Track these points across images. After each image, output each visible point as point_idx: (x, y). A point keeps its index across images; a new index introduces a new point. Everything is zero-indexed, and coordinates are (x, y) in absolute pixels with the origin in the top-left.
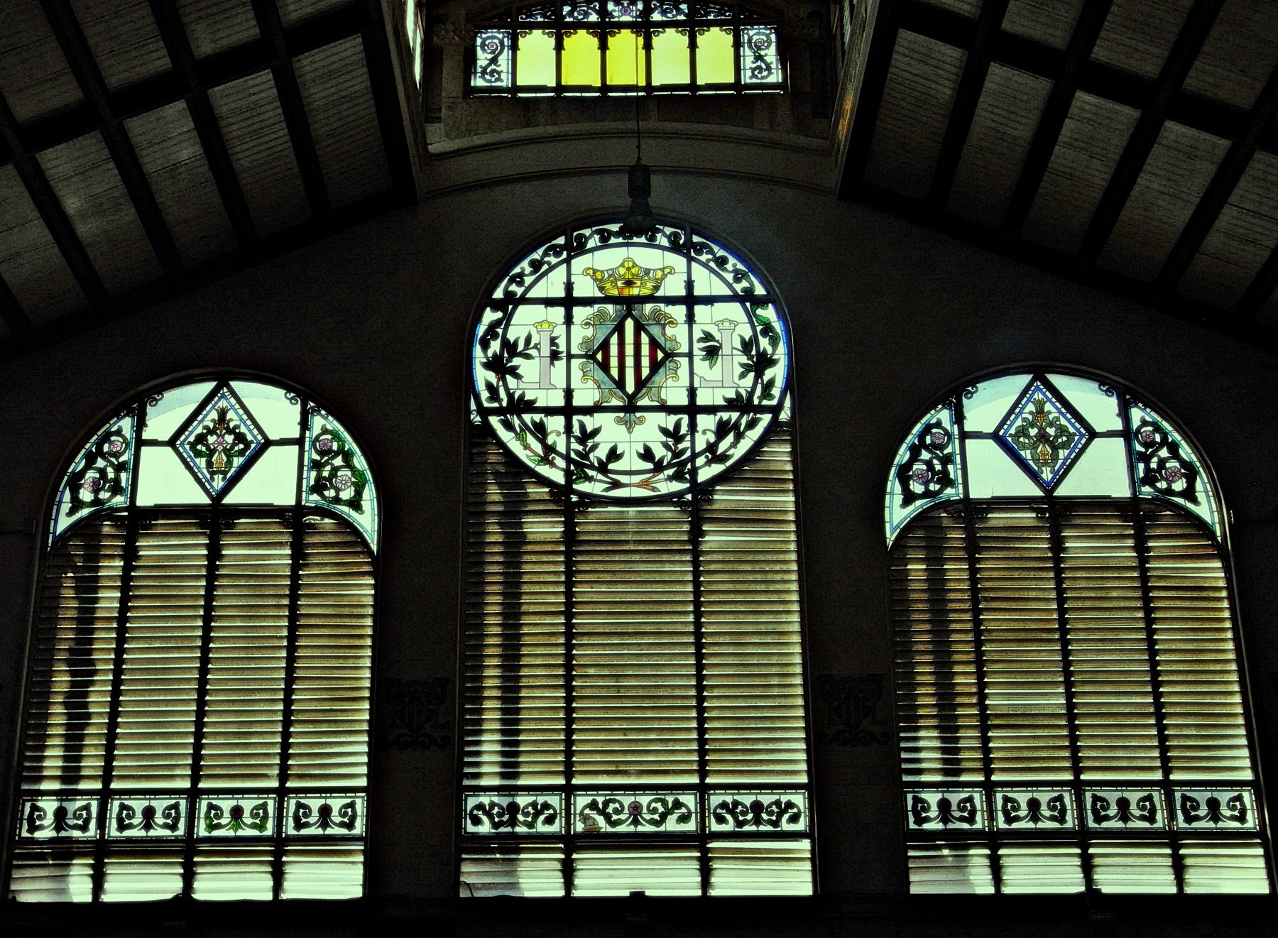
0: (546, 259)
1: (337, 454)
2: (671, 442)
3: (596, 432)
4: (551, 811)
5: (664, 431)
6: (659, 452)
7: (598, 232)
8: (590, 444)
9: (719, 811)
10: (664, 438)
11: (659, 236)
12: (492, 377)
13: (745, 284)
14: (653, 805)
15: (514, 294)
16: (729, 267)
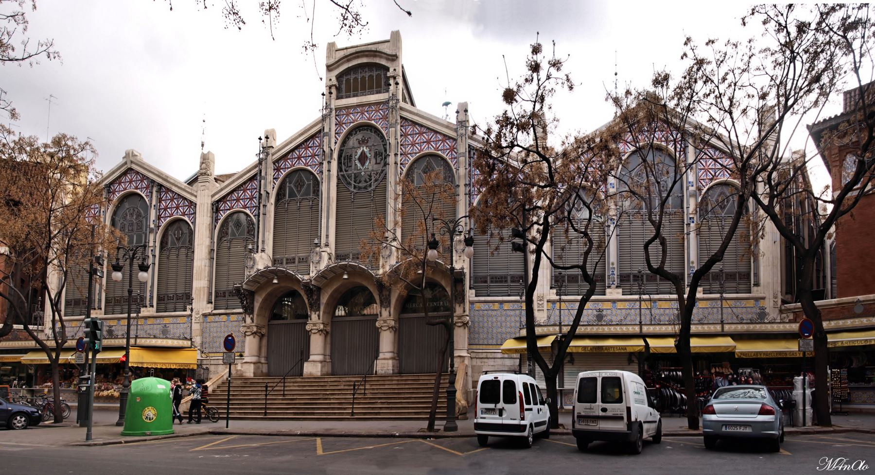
6: (368, 180)
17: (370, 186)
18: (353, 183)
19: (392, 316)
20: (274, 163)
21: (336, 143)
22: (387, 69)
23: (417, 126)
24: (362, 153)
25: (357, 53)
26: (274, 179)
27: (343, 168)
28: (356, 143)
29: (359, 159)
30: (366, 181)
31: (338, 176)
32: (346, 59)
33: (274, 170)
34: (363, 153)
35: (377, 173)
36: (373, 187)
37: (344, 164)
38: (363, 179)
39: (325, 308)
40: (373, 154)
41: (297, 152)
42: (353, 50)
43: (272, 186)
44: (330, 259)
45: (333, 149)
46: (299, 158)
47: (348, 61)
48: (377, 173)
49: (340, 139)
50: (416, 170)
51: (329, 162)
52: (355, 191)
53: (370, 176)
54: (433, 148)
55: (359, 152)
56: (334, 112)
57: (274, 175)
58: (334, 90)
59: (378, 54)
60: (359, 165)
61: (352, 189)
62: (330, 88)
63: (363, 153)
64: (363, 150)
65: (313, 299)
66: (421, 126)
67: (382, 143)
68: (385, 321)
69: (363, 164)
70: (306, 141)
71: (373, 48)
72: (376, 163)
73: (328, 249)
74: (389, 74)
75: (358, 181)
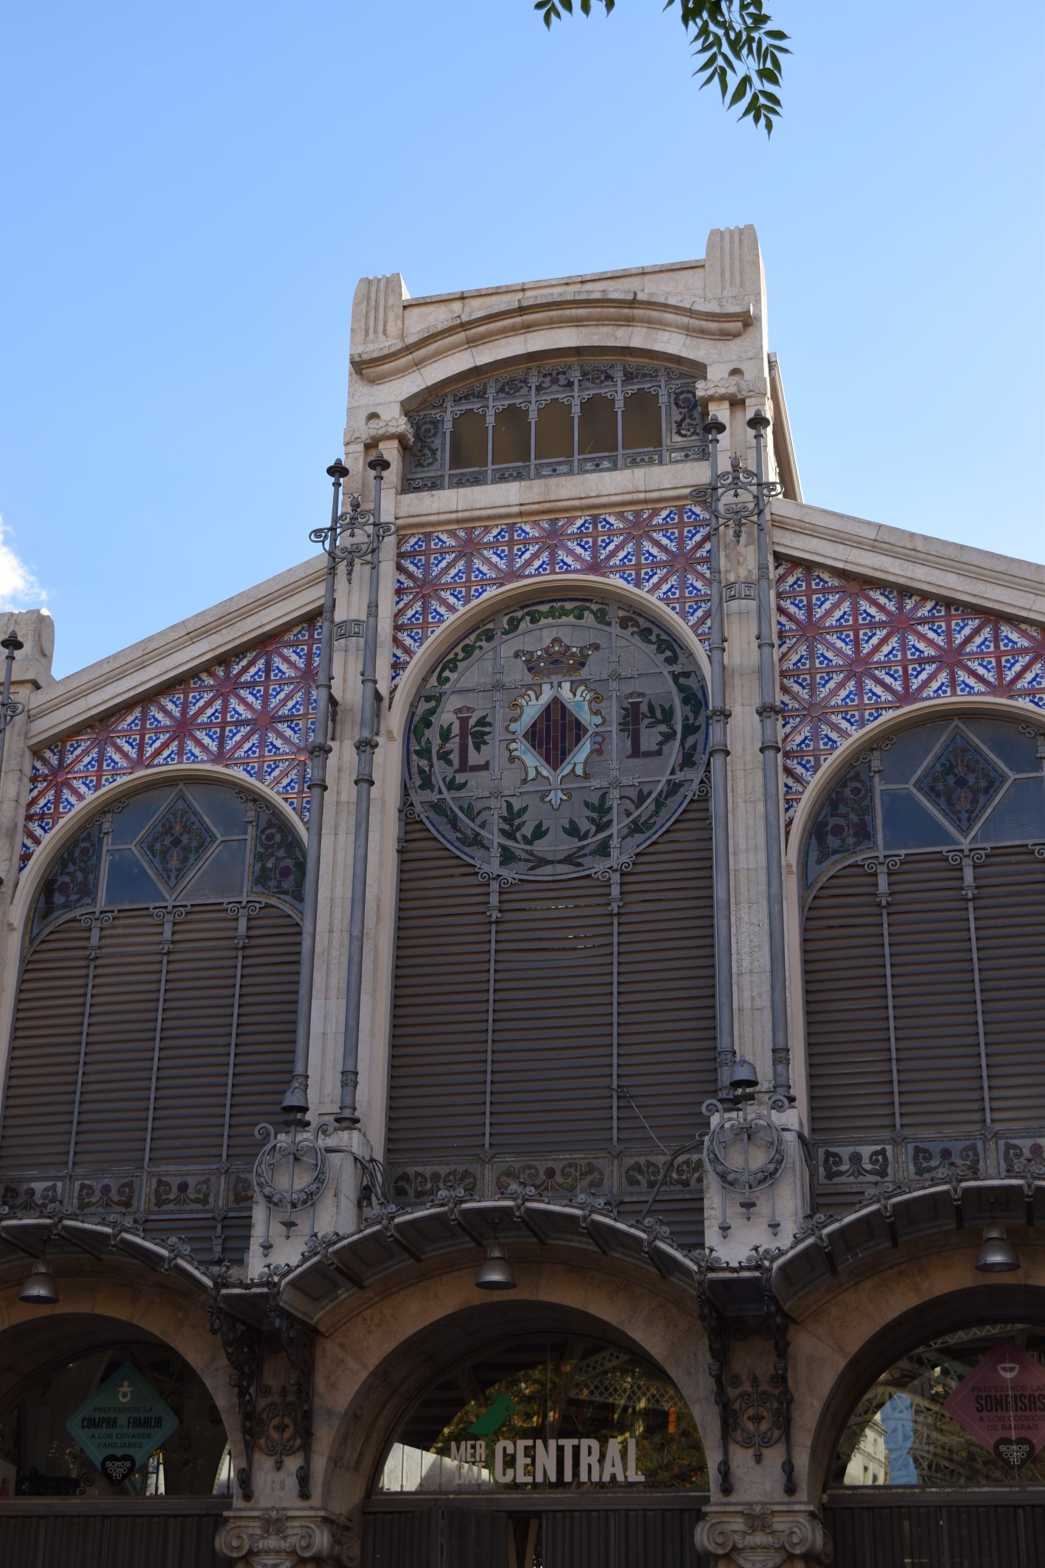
0: (479, 644)
1: (279, 847)
2: (595, 815)
3: (524, 810)
4: (471, 1180)
5: (587, 804)
6: (584, 826)
7: (528, 614)
8: (516, 822)
9: (631, 1173)
10: (589, 813)
11: (586, 613)
12: (423, 763)
13: (668, 653)
14: (567, 1169)
15: (447, 679)
16: (653, 638)
17: (603, 849)
18: (495, 838)
19: (803, 1495)
20: (36, 752)
21: (397, 667)
22: (699, 370)
23: (875, 595)
24: (548, 709)
25: (522, 310)
26: (29, 818)
27: (440, 771)
28: (517, 673)
29: (535, 736)
30: (573, 830)
31: (406, 808)
32: (461, 336)
33: (34, 780)
34: (556, 709)
35: (642, 798)
36: (618, 857)
37: (444, 757)
38: (555, 825)
39: (343, 1440)
40: (614, 714)
41: (170, 706)
42: (510, 302)
43: (19, 851)
44: (365, 1195)
45: (383, 688)
46: (183, 728)
47: (472, 343)
48: (642, 798)
49: (422, 654)
50: (879, 786)
51: (366, 746)
52: (509, 874)
53: (601, 808)
54: (980, 687)
55: (532, 709)
56: (390, 541)
57: (33, 802)
58: (390, 451)
59: (639, 312)
60: (532, 760)
61: (494, 867)
62: (370, 446)
63: (556, 709)
64: (556, 700)
65: (266, 1391)
66: (904, 592)
67: (666, 669)
68: (757, 1521)
69: (555, 755)
70: (224, 660)
71: (617, 291)
72: (636, 752)
73: (351, 1140)
74: (702, 389)
75: (527, 831)
